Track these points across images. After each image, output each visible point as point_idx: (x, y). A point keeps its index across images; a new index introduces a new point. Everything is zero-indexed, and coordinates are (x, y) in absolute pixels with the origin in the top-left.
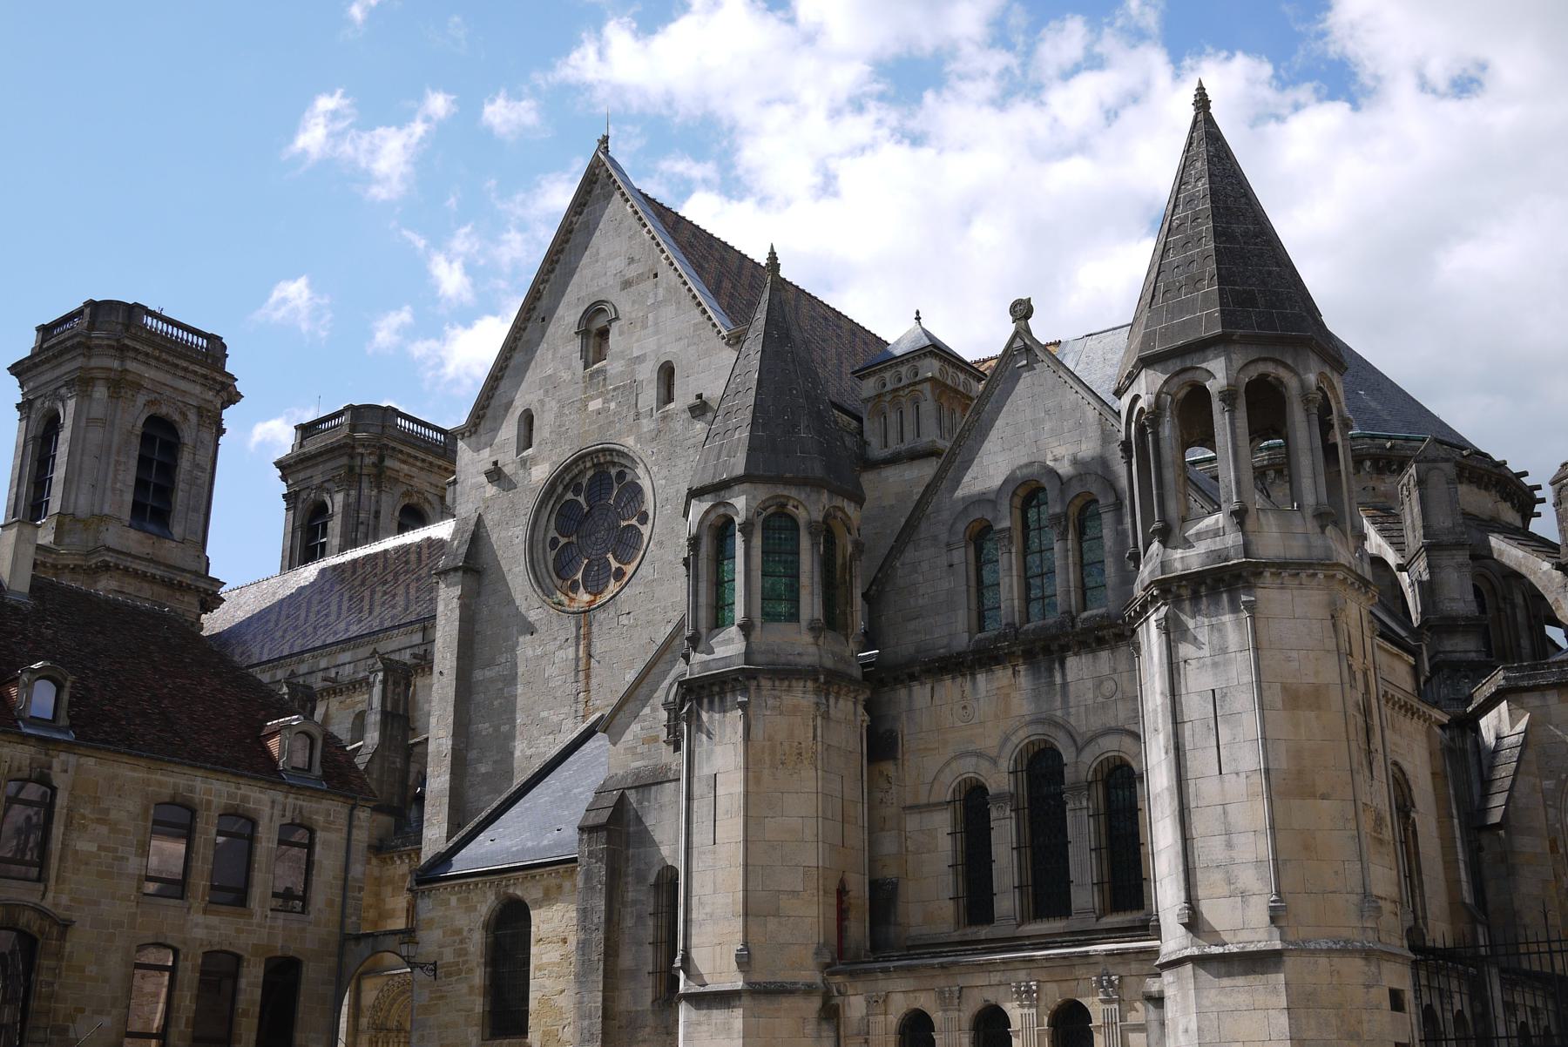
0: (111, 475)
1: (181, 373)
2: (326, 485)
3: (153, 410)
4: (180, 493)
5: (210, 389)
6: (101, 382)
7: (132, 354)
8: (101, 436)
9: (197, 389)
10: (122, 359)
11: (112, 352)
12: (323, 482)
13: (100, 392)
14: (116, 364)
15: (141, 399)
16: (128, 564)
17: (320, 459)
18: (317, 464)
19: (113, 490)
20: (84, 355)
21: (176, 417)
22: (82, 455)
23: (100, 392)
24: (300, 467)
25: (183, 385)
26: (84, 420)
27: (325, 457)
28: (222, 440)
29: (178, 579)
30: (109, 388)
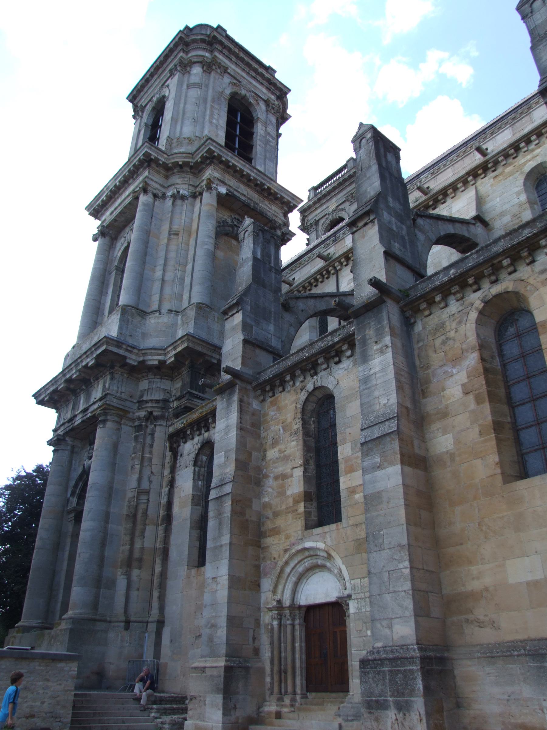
0: (208, 112)
1: (253, 74)
2: (340, 207)
3: (236, 89)
4: (258, 147)
5: (273, 93)
6: (197, 64)
7: (220, 48)
8: (199, 93)
9: (264, 90)
10: (211, 52)
11: (204, 45)
12: (337, 207)
13: (197, 70)
14: (207, 55)
15: (227, 79)
16: (229, 159)
17: (333, 193)
18: (331, 198)
19: (211, 122)
20: (184, 51)
21: (252, 100)
22: (185, 103)
23: (197, 70)
24: (318, 205)
25: (254, 83)
26: (185, 86)
27: (337, 191)
28: (280, 140)
29: (268, 185)
30: (203, 68)
